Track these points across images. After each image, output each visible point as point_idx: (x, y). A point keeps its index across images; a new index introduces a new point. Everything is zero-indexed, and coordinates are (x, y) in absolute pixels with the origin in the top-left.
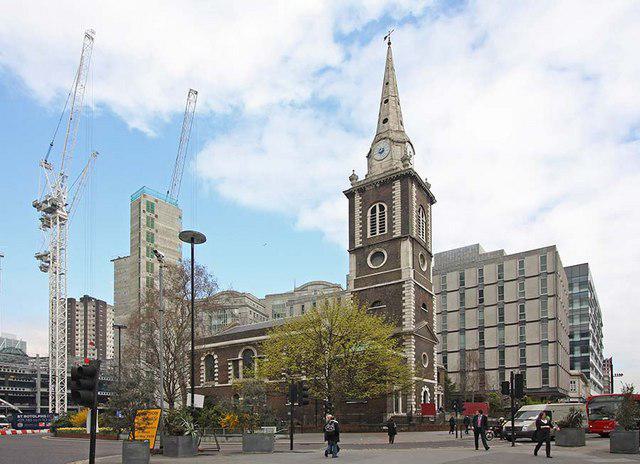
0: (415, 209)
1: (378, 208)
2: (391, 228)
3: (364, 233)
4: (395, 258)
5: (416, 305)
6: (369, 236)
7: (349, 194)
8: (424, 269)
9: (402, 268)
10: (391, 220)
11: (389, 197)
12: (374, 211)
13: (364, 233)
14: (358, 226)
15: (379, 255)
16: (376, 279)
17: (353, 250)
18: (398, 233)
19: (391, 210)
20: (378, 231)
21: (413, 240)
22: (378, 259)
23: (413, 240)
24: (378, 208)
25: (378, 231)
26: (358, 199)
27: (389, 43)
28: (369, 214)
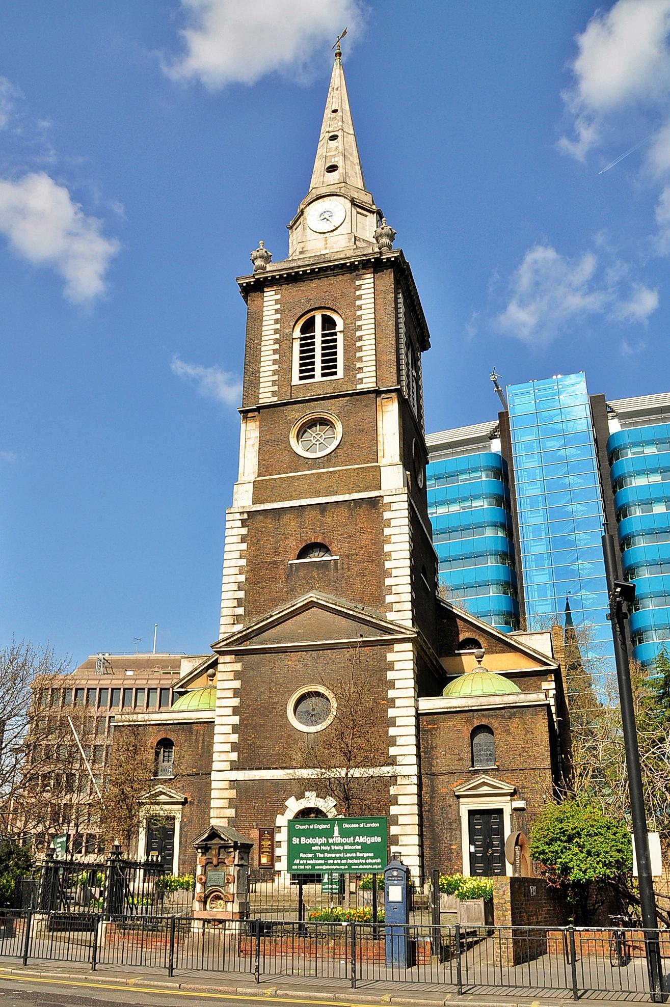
3: (284, 371)
6: (296, 381)
9: (382, 462)
10: (352, 349)
12: (309, 326)
18: (369, 383)
20: (318, 371)
21: (404, 405)
25: (318, 371)
28: (297, 333)
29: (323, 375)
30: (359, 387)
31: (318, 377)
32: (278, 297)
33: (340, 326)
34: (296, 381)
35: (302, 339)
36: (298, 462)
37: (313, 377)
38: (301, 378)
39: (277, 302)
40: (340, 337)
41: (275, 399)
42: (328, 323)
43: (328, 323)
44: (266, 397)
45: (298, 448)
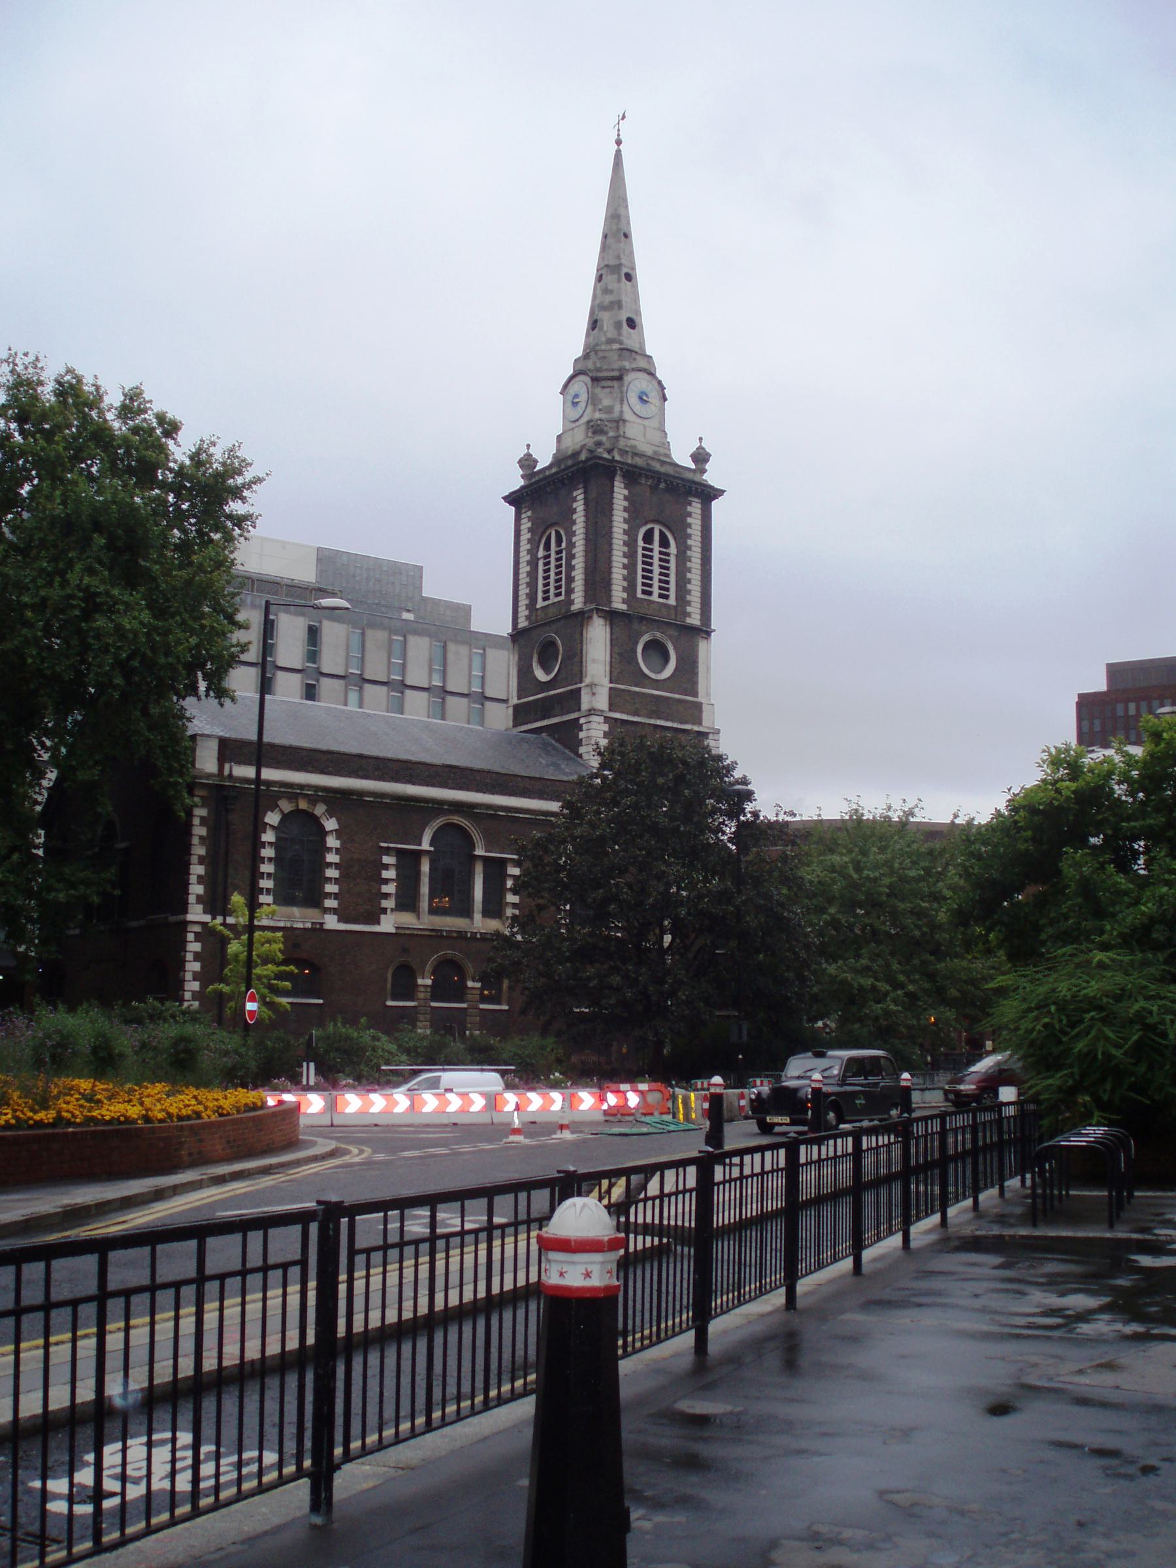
3: (630, 580)
6: (639, 595)
11: (612, 501)
12: (648, 538)
16: (658, 707)
18: (695, 620)
19: (682, 558)
20: (656, 591)
22: (656, 659)
25: (656, 591)
27: (619, 142)
28: (641, 543)
29: (661, 596)
31: (655, 597)
32: (626, 492)
33: (673, 549)
36: (642, 679)
39: (626, 498)
40: (673, 559)
41: (624, 607)
42: (664, 543)
43: (664, 543)
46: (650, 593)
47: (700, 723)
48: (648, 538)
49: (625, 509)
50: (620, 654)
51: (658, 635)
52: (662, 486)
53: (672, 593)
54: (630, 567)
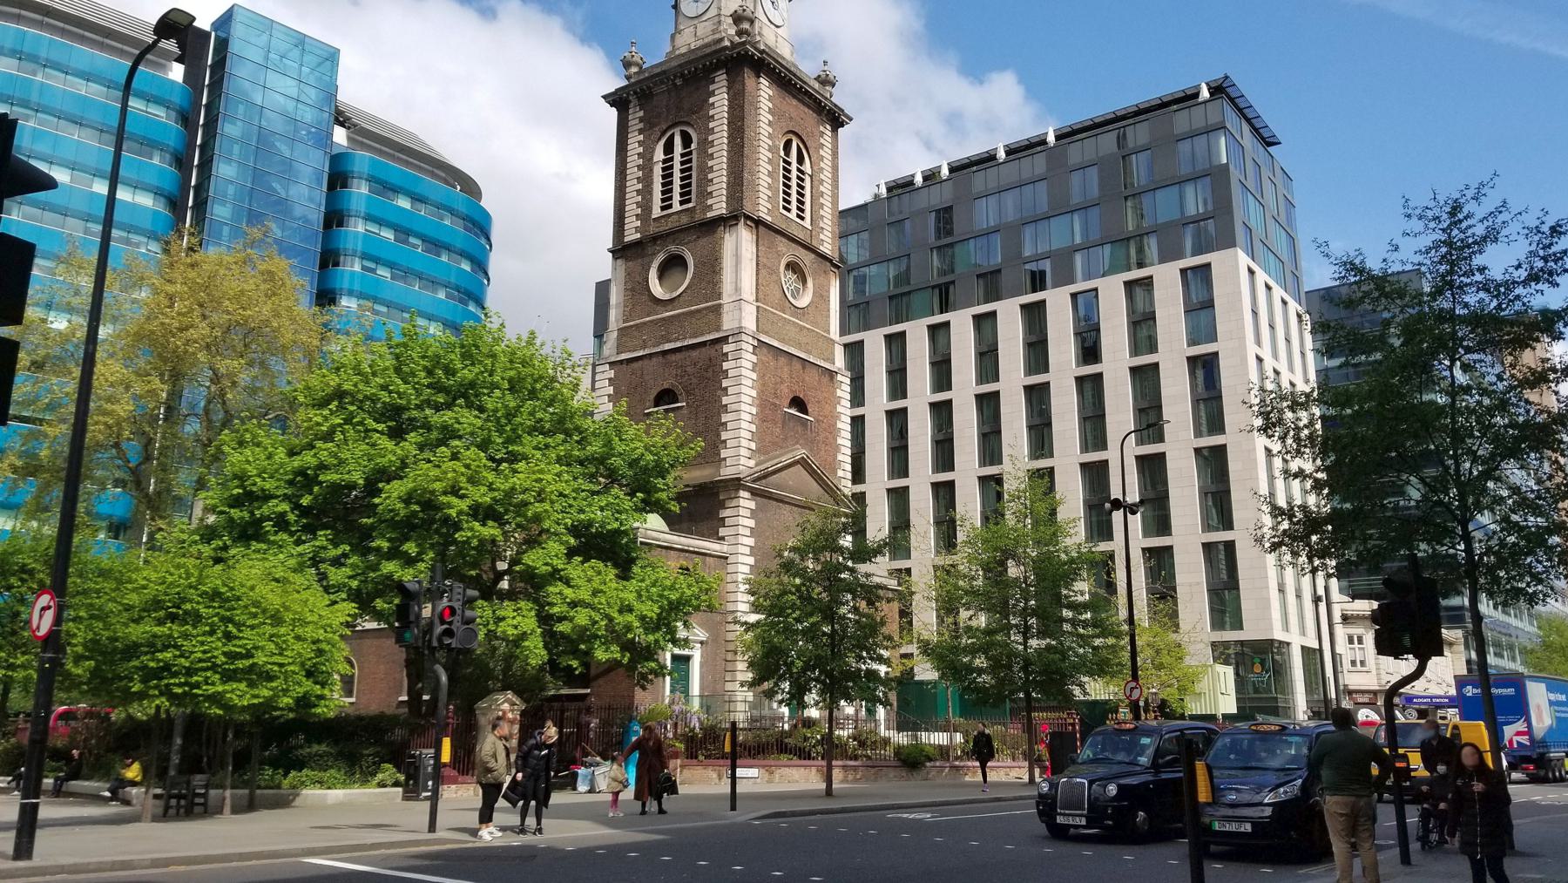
0: (765, 142)
1: (678, 140)
2: (705, 194)
3: (646, 206)
4: (711, 269)
5: (766, 406)
6: (657, 212)
7: (617, 100)
8: (804, 301)
9: (725, 299)
12: (669, 148)
13: (646, 206)
14: (633, 186)
15: (673, 264)
17: (622, 250)
18: (719, 207)
20: (677, 198)
22: (675, 274)
23: (758, 223)
24: (678, 140)
25: (677, 198)
26: (635, 114)
28: (659, 155)
30: (709, 215)
31: (677, 207)
34: (657, 212)
35: (664, 161)
37: (670, 206)
38: (663, 208)
40: (694, 156)
42: (687, 140)
44: (631, 236)
45: (657, 289)
46: (670, 206)
47: (718, 329)
48: (669, 148)
49: (641, 131)
50: (633, 290)
51: (673, 248)
52: (679, 82)
53: (693, 196)
54: (646, 192)
